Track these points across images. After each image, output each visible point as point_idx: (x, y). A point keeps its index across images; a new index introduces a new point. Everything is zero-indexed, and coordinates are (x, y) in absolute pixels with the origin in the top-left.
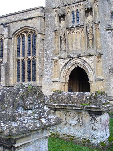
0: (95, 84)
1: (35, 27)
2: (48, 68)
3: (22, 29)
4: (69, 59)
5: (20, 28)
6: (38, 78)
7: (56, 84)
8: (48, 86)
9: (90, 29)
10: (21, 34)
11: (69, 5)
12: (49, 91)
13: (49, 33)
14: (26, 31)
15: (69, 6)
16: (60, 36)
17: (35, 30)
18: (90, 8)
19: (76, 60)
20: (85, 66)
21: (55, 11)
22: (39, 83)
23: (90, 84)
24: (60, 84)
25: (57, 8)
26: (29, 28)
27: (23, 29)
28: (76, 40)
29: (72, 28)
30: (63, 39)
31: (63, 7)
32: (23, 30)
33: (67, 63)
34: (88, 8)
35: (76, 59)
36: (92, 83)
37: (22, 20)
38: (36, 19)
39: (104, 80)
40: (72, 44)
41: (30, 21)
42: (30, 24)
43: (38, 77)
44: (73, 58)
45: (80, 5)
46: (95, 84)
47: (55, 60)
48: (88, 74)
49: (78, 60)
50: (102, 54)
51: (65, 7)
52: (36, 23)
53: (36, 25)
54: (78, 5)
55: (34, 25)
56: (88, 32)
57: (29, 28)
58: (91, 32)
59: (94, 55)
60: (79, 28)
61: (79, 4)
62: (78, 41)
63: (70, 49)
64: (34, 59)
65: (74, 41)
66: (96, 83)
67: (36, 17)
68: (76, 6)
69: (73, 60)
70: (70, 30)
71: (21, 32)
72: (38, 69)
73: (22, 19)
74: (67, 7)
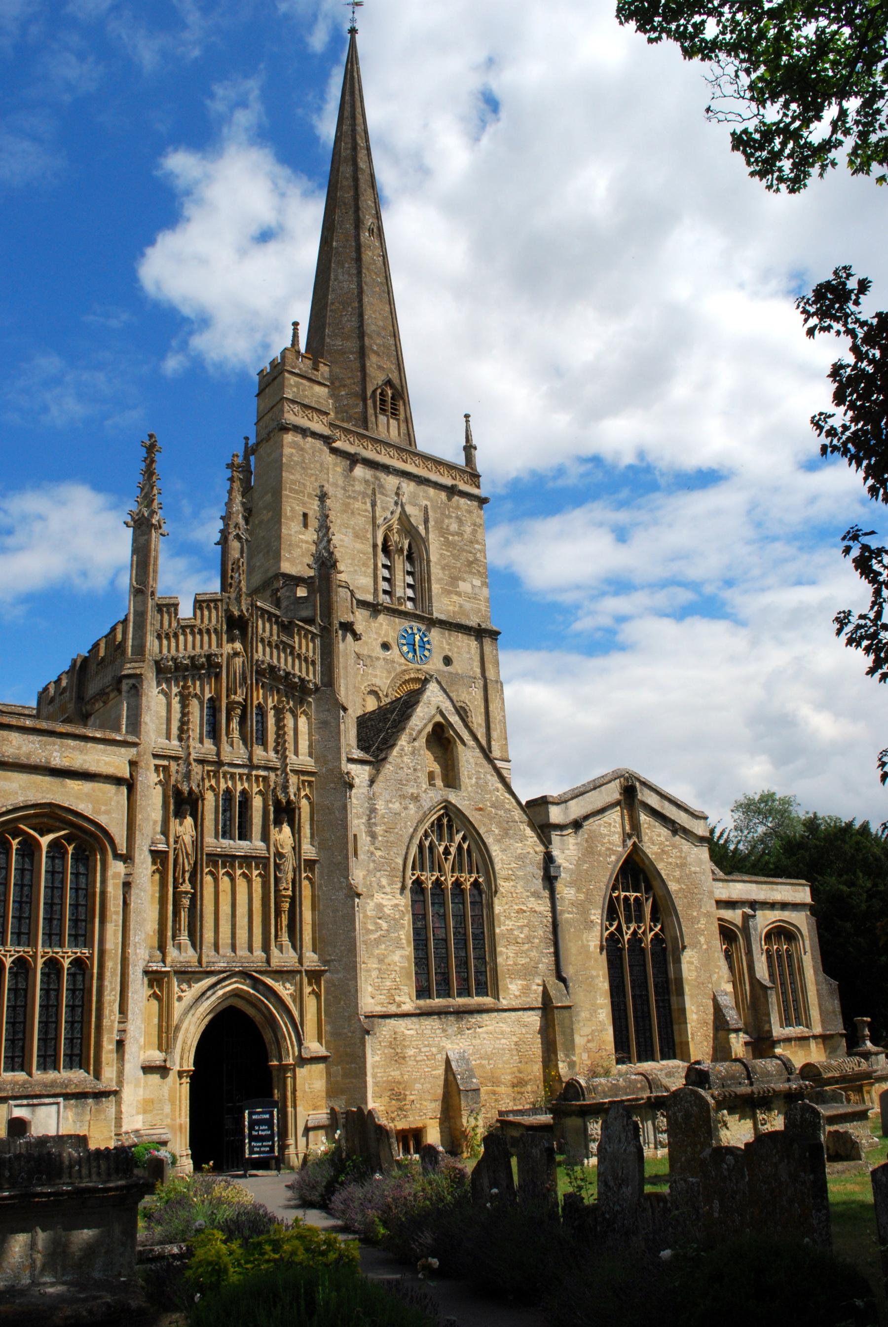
1: (102, 820)
4: (212, 980)
6: (111, 1052)
7: (155, 1078)
10: (17, 833)
12: (134, 1112)
23: (275, 1073)
29: (226, 856)
30: (186, 893)
38: (110, 789)
42: (77, 798)
48: (268, 1036)
51: (200, 767)
52: (106, 805)
53: (107, 812)
55: (97, 811)
68: (241, 775)
73: (34, 760)
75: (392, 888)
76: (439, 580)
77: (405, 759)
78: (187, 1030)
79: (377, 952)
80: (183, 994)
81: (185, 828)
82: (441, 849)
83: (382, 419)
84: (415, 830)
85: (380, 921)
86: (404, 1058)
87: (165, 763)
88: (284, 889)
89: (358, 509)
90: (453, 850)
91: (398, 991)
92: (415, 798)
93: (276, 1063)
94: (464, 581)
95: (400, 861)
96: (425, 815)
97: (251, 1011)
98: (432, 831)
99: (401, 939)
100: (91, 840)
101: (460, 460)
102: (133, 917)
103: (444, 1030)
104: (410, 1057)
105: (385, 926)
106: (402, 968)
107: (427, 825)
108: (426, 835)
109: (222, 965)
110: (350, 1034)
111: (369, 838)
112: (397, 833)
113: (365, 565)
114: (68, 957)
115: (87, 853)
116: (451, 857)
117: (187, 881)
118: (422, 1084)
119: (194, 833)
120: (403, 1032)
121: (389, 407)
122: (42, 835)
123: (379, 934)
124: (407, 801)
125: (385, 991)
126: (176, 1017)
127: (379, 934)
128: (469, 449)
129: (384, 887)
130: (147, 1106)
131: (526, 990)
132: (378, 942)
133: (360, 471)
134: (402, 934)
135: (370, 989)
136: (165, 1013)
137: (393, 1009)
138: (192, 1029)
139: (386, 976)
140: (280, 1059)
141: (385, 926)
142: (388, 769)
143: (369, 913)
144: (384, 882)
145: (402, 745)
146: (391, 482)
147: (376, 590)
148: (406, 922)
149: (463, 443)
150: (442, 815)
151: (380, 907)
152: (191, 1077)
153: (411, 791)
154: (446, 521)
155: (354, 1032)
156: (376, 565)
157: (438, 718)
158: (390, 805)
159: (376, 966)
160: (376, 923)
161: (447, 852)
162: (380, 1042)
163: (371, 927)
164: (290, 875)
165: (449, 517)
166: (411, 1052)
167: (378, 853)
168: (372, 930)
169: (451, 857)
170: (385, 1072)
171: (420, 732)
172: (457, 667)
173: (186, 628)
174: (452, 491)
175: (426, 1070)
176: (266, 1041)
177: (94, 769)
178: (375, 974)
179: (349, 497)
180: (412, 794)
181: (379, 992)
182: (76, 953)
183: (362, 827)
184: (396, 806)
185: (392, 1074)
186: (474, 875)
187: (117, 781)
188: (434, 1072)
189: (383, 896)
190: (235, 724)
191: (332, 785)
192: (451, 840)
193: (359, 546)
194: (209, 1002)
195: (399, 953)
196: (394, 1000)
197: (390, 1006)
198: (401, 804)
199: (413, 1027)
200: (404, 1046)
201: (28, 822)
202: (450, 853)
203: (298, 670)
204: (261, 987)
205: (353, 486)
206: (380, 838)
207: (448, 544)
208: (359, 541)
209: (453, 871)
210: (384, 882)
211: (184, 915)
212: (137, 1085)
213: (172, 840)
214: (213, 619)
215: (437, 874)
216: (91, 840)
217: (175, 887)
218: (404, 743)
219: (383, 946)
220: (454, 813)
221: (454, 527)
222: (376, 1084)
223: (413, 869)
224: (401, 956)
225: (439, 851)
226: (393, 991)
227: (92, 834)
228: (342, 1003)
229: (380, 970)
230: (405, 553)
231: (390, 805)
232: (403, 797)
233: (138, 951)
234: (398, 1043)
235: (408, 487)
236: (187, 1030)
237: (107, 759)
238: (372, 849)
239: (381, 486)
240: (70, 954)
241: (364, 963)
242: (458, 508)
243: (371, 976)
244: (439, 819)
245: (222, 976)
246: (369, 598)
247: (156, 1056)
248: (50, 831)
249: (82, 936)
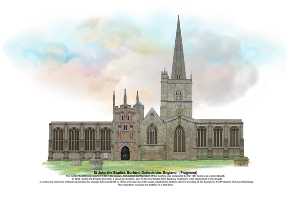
81: (120, 129)
131: (161, 144)
136: (118, 146)
146: (177, 85)
172: (186, 107)
173: (119, 108)
174: (187, 83)
207: (186, 91)
214: (123, 107)
235: (180, 85)
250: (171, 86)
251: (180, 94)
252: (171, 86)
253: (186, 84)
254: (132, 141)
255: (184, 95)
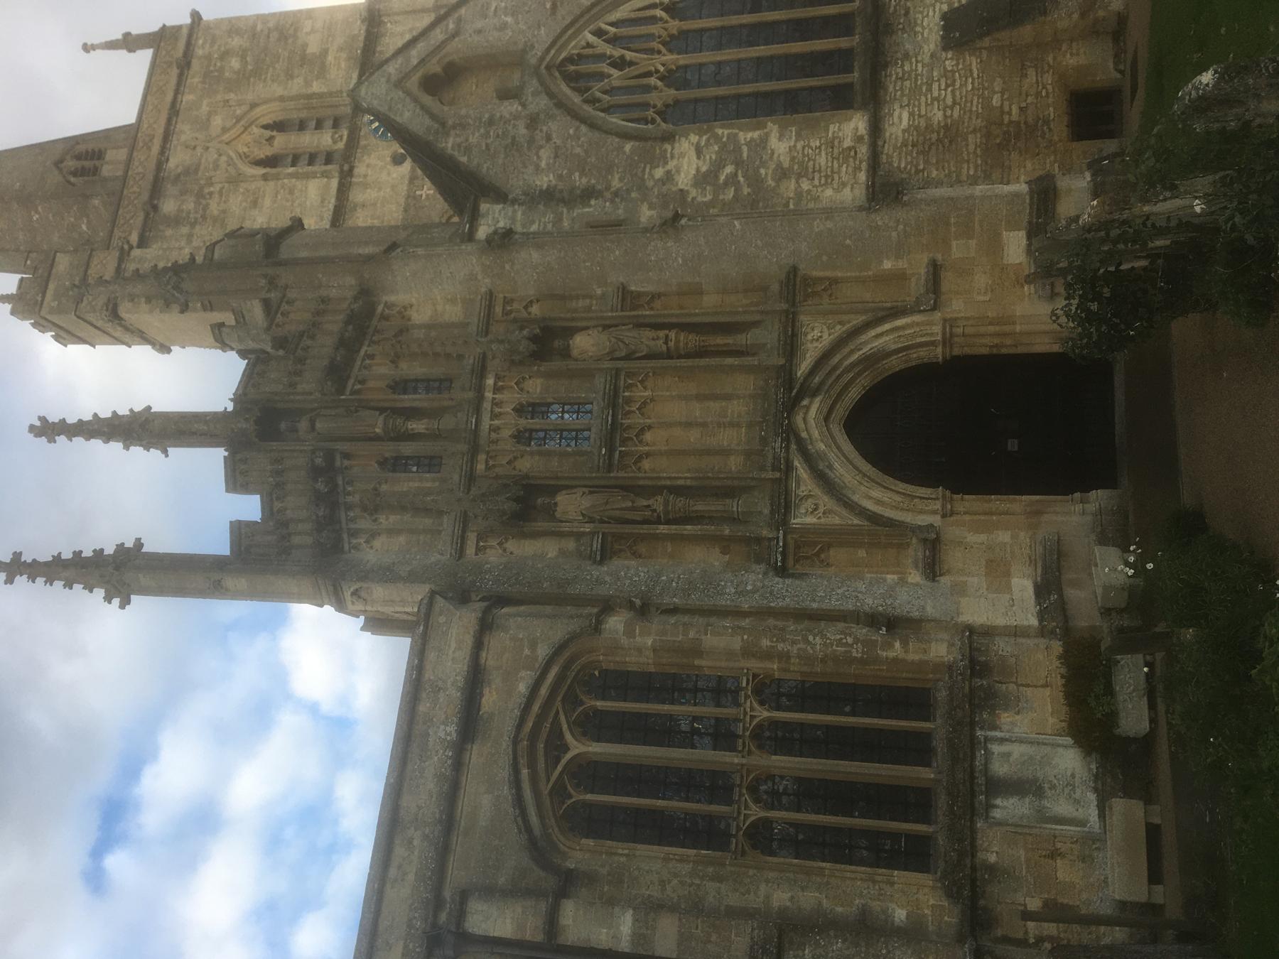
0: (956, 307)
1: (543, 651)
2: (839, 591)
3: (525, 772)
5: (506, 791)
6: (905, 644)
7: (953, 558)
8: (964, 601)
9: (648, 340)
10: (559, 792)
11: (474, 450)
12: (1008, 596)
13: (607, 579)
14: (546, 747)
15: (482, 457)
16: (645, 522)
17: (566, 654)
18: (533, 347)
19: (805, 419)
20: (853, 365)
21: (479, 550)
22: (945, 645)
23: (956, 352)
24: (953, 531)
25: (464, 531)
26: (536, 708)
27: (523, 761)
28: (689, 425)
30: (666, 503)
31: (473, 489)
32: (532, 765)
33: (822, 478)
34: (534, 339)
35: (799, 420)
36: (951, 327)
37: (458, 764)
39: (939, 257)
40: (708, 452)
41: (490, 700)
43: (897, 645)
44: (790, 434)
45: (497, 389)
46: (960, 311)
47: (790, 562)
48: (895, 364)
49: (808, 408)
50: (795, 269)
53: (533, 646)
54: (495, 403)
56: (660, 346)
57: (536, 708)
58: (662, 334)
59: (794, 313)
60: (628, 401)
61: (489, 395)
62: (697, 410)
63: (735, 464)
64: (766, 690)
65: (694, 436)
66: (954, 302)
67: (478, 645)
68: (494, 416)
69: (804, 435)
70: (622, 454)
71: (545, 789)
72: (839, 643)
74: (481, 467)
75: (672, 157)
76: (308, 83)
77: (473, 140)
78: (879, 502)
79: (771, 182)
80: (821, 509)
81: (571, 505)
82: (615, 73)
83: (106, 171)
84: (583, 120)
85: (722, 178)
86: (947, 128)
87: (472, 538)
88: (666, 343)
89: (218, 204)
90: (617, 53)
91: (836, 143)
92: (533, 122)
93: (939, 350)
94: (305, 45)
95: (628, 147)
96: (561, 105)
97: (854, 394)
98: (588, 89)
99: (752, 139)
100: (576, 667)
101: (145, 56)
102: (695, 599)
103: (907, 56)
104: (945, 116)
105: (729, 169)
106: (799, 137)
107: (577, 99)
108: (592, 101)
109: (778, 445)
110: (901, 227)
111: (593, 202)
112: (586, 152)
113: (291, 192)
114: (752, 709)
115: (597, 673)
116: (629, 55)
117: (650, 502)
118: (995, 93)
119: (580, 491)
120: (904, 131)
121: (88, 164)
122: (566, 748)
123: (741, 179)
124: (539, 136)
125: (836, 165)
126: (856, 522)
127: (741, 179)
128: (130, 43)
129: (668, 172)
130: (997, 571)
132: (756, 182)
133: (168, 206)
134: (745, 136)
135: (829, 192)
137: (863, 150)
138: (877, 493)
139: (811, 163)
140: (933, 343)
141: (729, 169)
142: (488, 169)
143: (709, 197)
144: (659, 173)
145: (453, 148)
146: (177, 159)
147: (325, 175)
148: (726, 132)
149: (123, 53)
150: (560, 73)
151: (702, 180)
152: (955, 492)
153: (523, 131)
154: (227, 74)
155: (898, 221)
156: (291, 176)
157: (413, 83)
158: (543, 164)
159: (793, 181)
160: (726, 184)
161: (620, 64)
162: (917, 172)
163: (730, 193)
164: (649, 333)
165: (221, 70)
166: (938, 116)
167: (616, 183)
168: (736, 190)
169: (629, 55)
170: (968, 162)
171: (433, 116)
175: (970, 87)
176: (903, 367)
177: (465, 668)
178: (805, 185)
179: (204, 217)
180: (527, 127)
181: (836, 177)
182: (747, 697)
183: (577, 212)
184: (545, 154)
185: (971, 148)
186: (659, 13)
187: (485, 626)
188: (975, 75)
189: (682, 175)
190: (418, 426)
191: (507, 267)
192: (601, 57)
193: (267, 202)
194: (836, 465)
195: (774, 142)
196: (850, 149)
197: (859, 155)
198: (541, 147)
199: (896, 114)
200: (926, 128)
201: (542, 775)
202: (622, 57)
203: (334, 324)
204: (817, 380)
205: (189, 213)
206: (593, 181)
208: (260, 200)
209: (651, 51)
210: (659, 173)
211: (700, 507)
212: (960, 590)
213: (587, 528)
215: (653, 81)
216: (576, 667)
217: (659, 522)
218: (450, 145)
219: (763, 171)
220: (559, 51)
221: (235, 63)
222: (987, 178)
223: (646, 121)
224: (780, 139)
225: (618, 78)
226: (836, 151)
227: (566, 668)
228: (848, 241)
229: (799, 176)
230: (274, 133)
231: (543, 164)
232: (531, 141)
233: (749, 588)
234: (921, 138)
235: (185, 131)
236: (879, 502)
237: (453, 645)
238: (608, 195)
239: (187, 172)
240: (748, 703)
241: (787, 205)
242: (208, 57)
243: (809, 192)
244: (571, 79)
245: (793, 447)
246: (334, 183)
247: (915, 551)
248: (561, 735)
249: (722, 690)
250: (176, 221)
251: (280, 126)
252: (176, 221)
253: (194, 80)
254: (768, 336)
255: (296, 86)
